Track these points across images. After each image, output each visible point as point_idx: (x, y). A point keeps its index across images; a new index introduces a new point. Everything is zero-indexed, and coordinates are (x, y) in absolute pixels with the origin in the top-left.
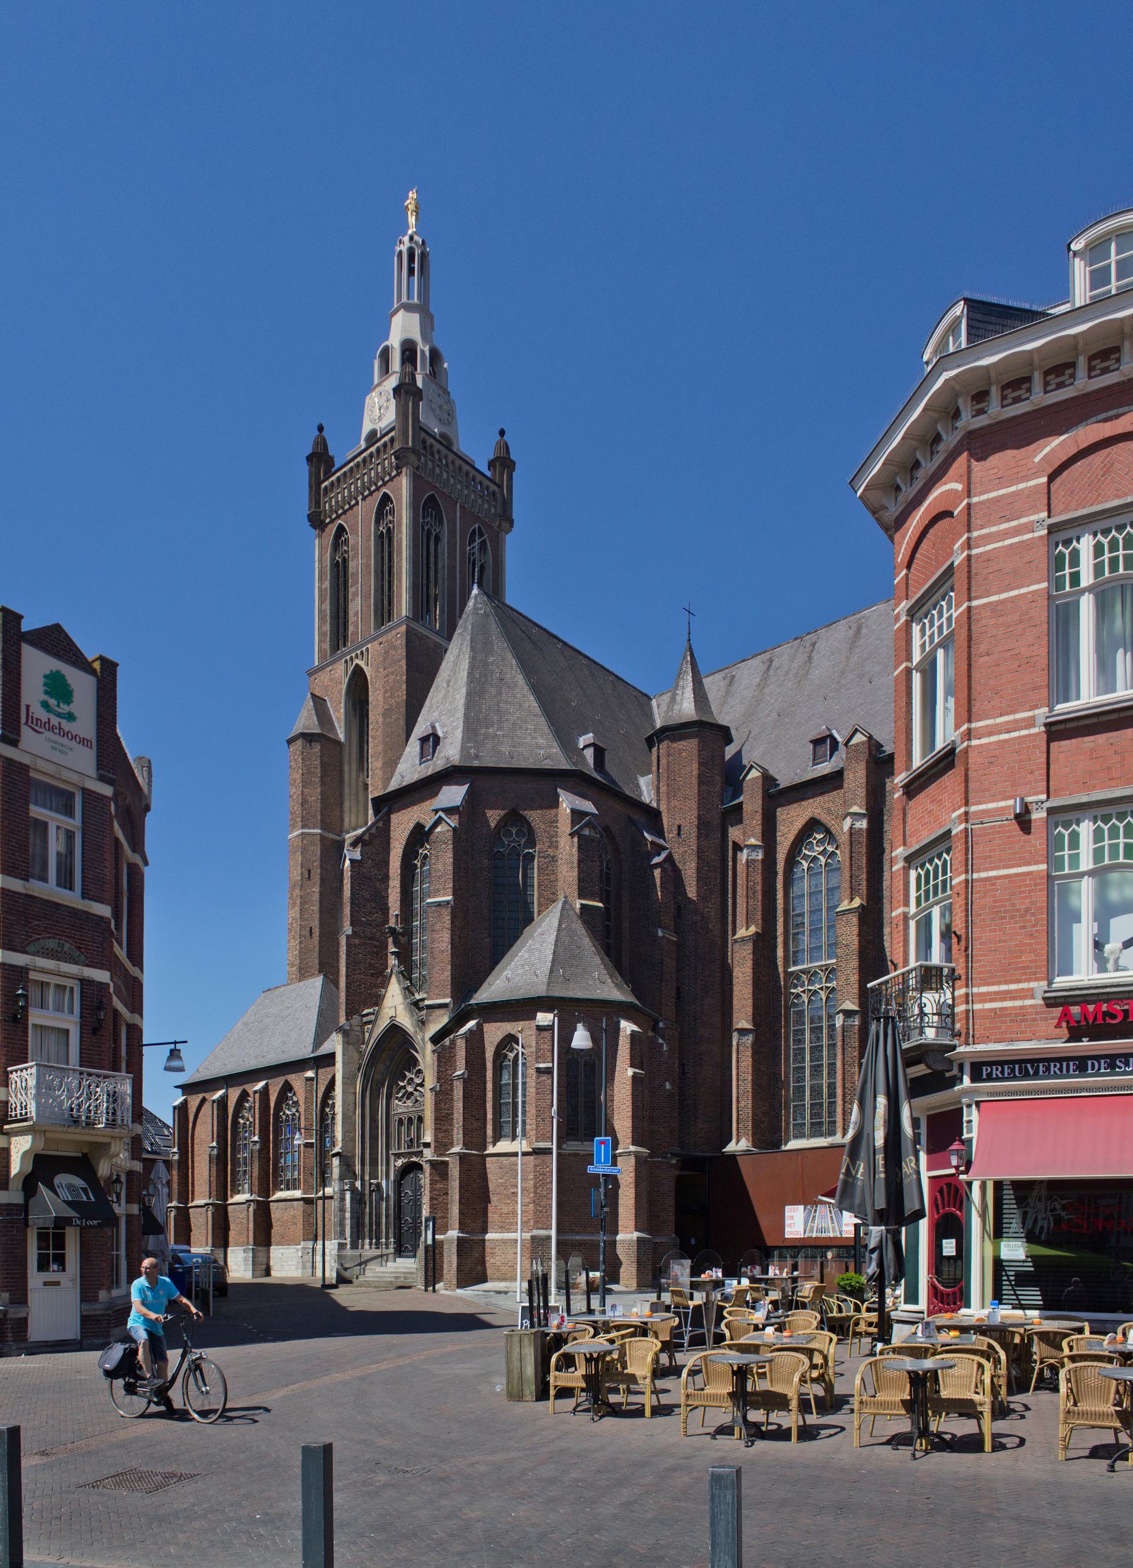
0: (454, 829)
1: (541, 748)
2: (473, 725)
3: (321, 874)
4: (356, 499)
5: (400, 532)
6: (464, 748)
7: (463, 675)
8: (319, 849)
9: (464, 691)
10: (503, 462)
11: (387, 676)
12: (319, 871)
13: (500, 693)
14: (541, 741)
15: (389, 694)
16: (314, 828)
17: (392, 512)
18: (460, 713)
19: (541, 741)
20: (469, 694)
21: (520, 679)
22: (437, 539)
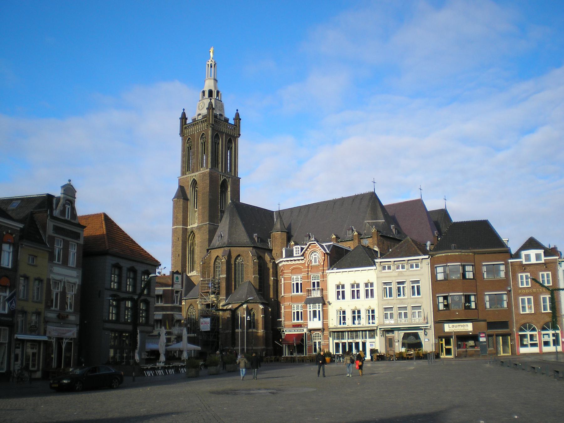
0: (226, 261)
1: (245, 240)
2: (230, 234)
3: (182, 239)
4: (194, 132)
5: (208, 144)
6: (228, 241)
7: (228, 222)
8: (181, 232)
9: (228, 227)
10: (237, 118)
11: (203, 183)
12: (181, 238)
13: (236, 227)
14: (245, 238)
15: (203, 189)
16: (180, 225)
17: (205, 137)
18: (227, 232)
19: (245, 238)
20: (229, 227)
21: (241, 223)
22: (218, 144)
